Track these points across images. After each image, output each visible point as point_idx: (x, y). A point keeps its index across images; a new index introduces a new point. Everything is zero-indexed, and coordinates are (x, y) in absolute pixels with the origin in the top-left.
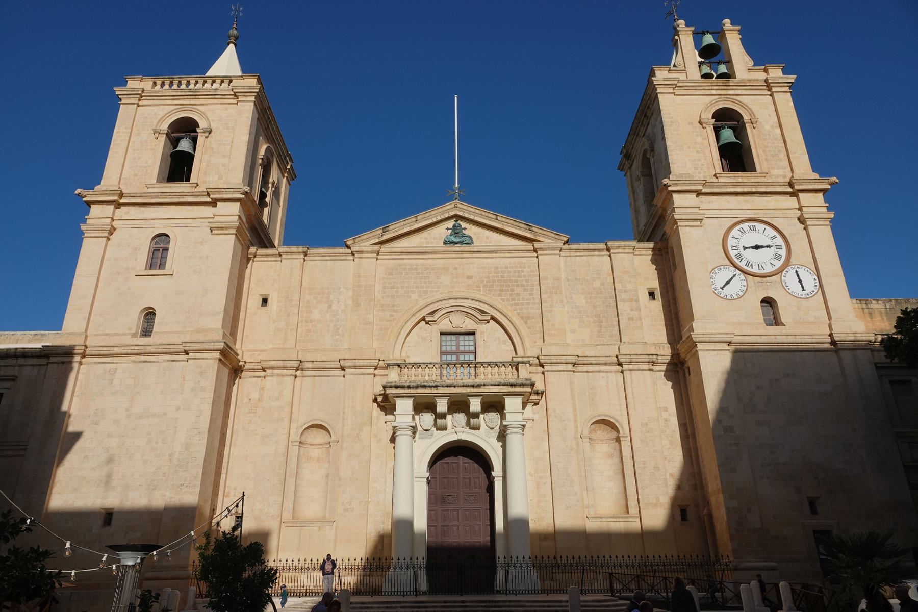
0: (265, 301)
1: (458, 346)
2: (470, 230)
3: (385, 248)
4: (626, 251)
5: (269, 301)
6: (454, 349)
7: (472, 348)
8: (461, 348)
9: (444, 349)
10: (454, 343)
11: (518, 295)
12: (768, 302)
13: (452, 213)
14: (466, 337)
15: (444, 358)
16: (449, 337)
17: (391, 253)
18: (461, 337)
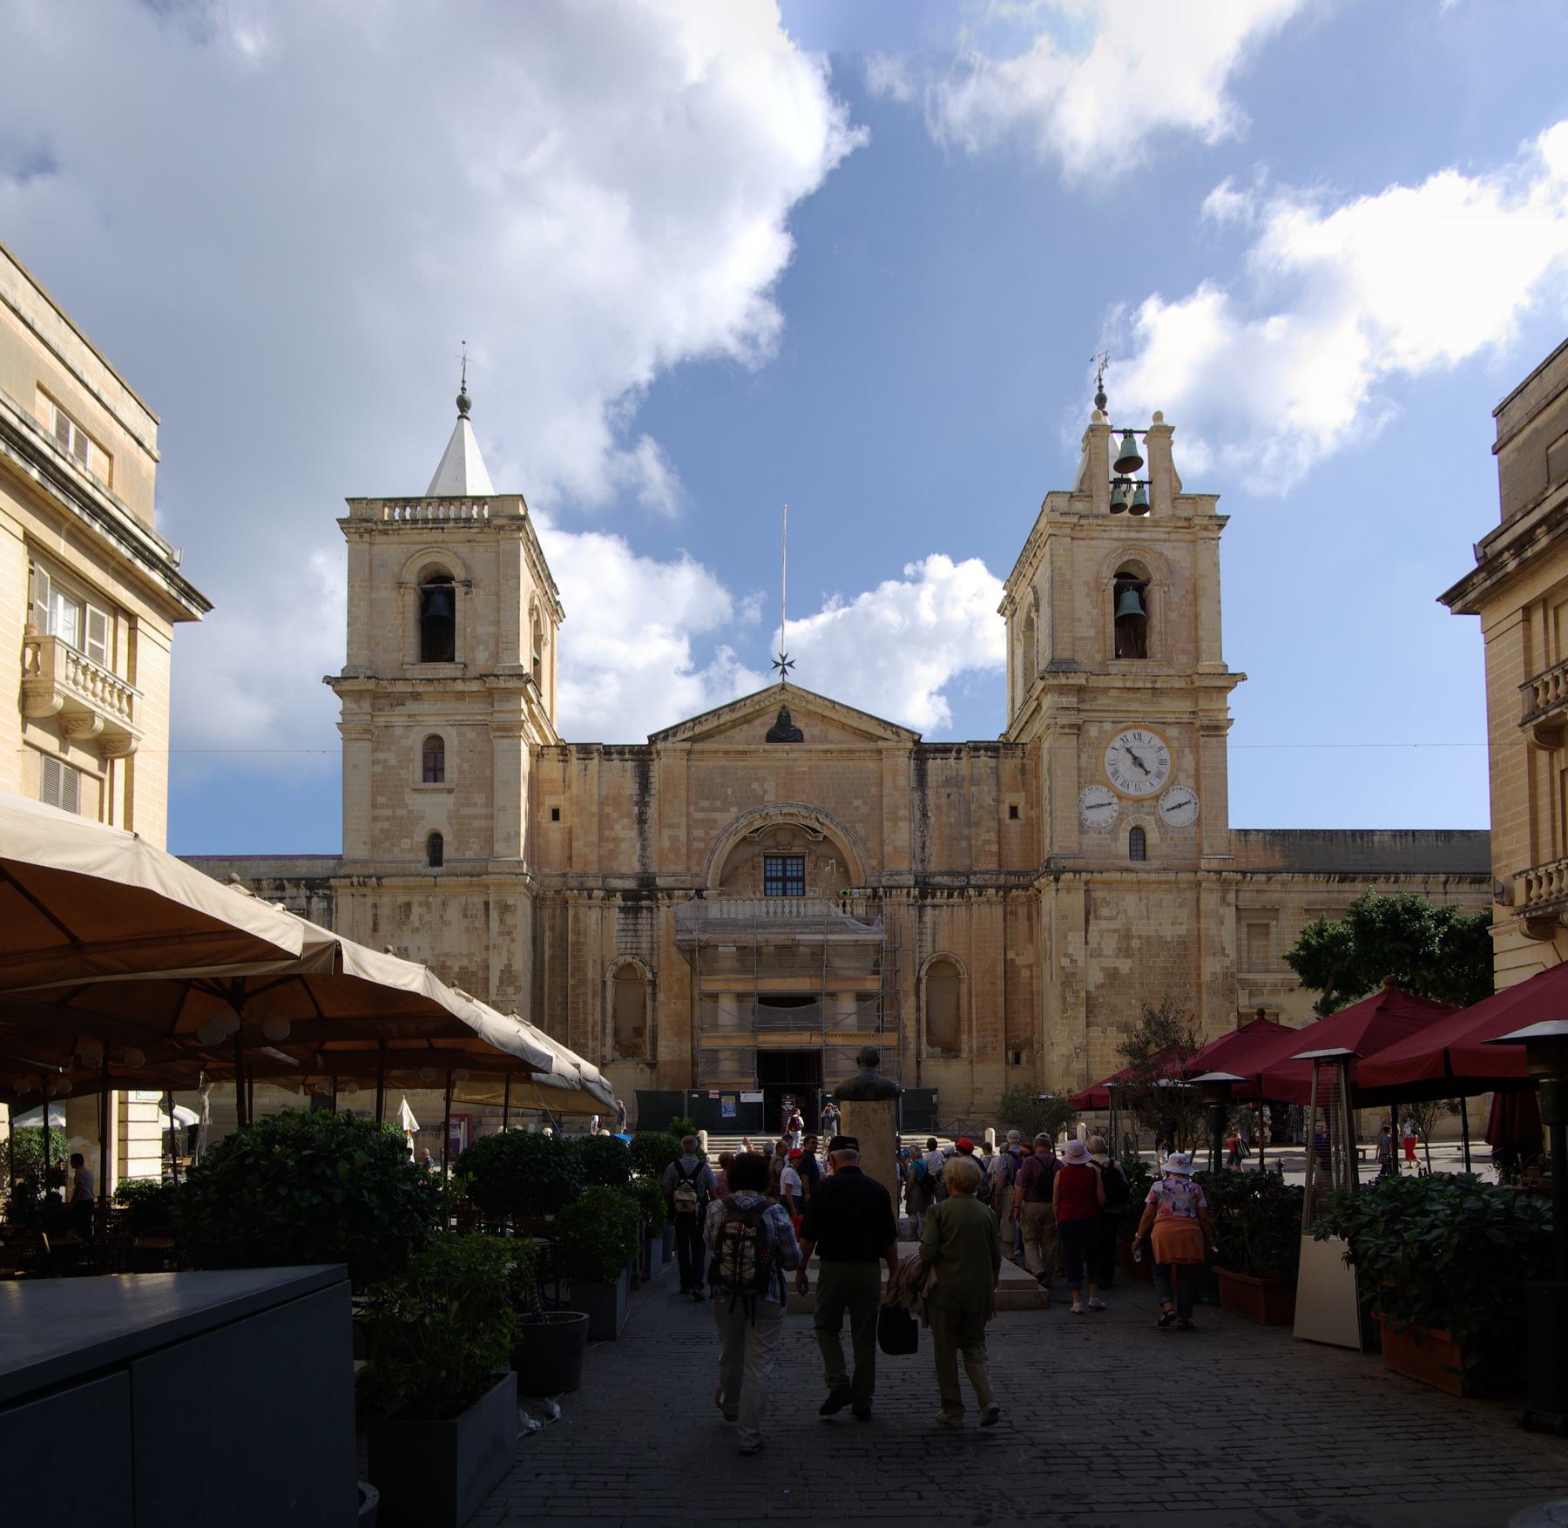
0: (556, 815)
1: (784, 871)
2: (799, 723)
3: (698, 746)
4: (989, 754)
5: (561, 814)
6: (780, 874)
7: (800, 874)
8: (789, 874)
9: (768, 874)
10: (780, 868)
11: (857, 808)
12: (1138, 834)
13: (778, 698)
14: (795, 861)
15: (769, 885)
16: (774, 861)
17: (703, 752)
18: (789, 861)
